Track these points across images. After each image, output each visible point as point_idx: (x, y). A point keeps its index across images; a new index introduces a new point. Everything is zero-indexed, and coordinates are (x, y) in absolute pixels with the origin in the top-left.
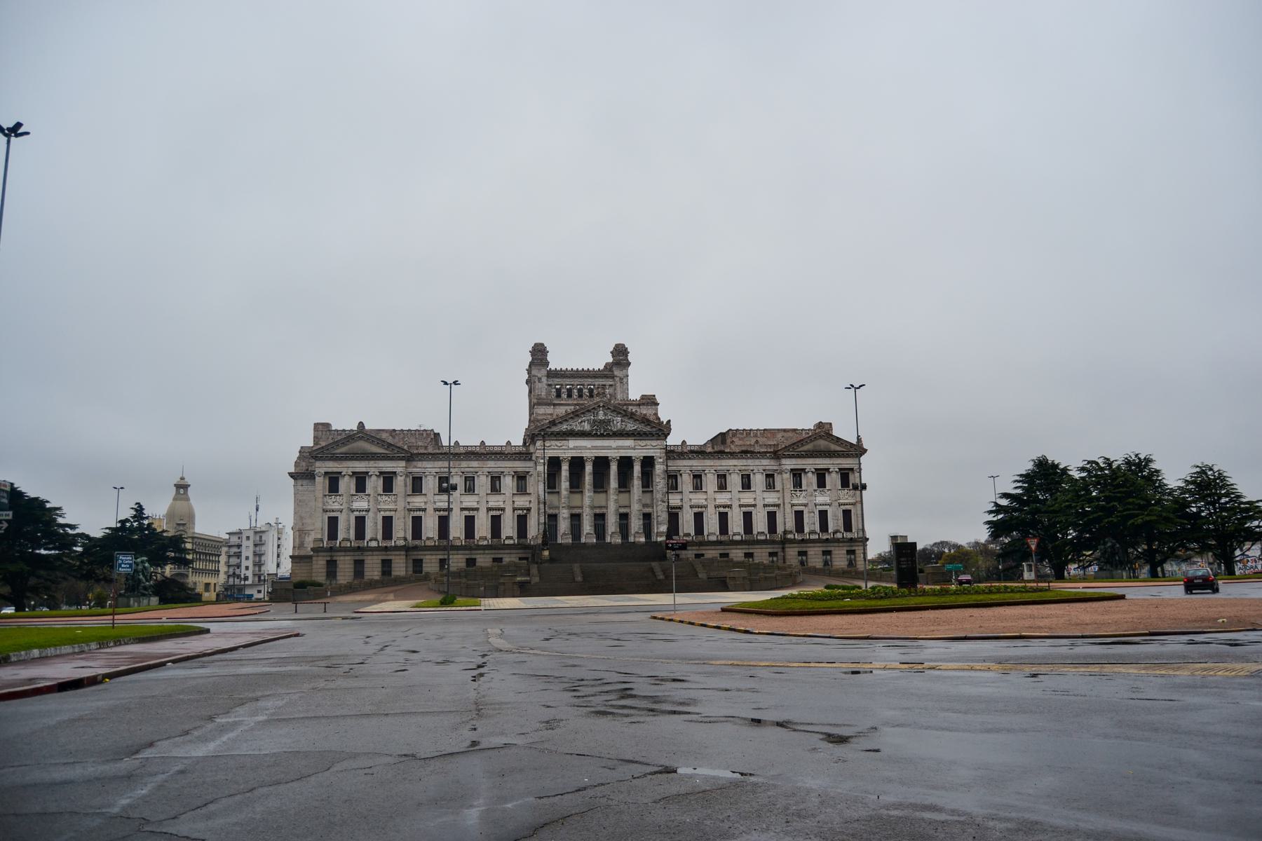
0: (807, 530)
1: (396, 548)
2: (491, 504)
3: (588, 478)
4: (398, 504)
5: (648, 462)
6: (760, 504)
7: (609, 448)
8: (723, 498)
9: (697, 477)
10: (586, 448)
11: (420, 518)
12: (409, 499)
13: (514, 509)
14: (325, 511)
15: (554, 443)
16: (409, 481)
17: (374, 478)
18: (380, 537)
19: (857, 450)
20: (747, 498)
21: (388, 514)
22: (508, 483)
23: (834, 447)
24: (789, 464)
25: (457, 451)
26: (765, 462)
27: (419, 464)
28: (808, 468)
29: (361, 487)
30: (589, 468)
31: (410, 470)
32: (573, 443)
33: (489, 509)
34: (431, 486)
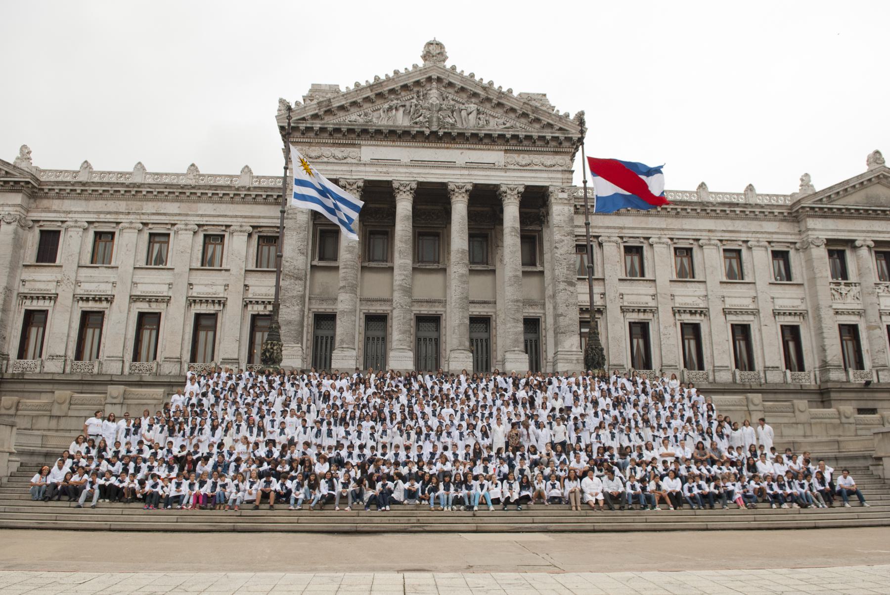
2: (197, 291)
3: (403, 227)
5: (535, 202)
6: (766, 310)
7: (450, 165)
8: (688, 295)
9: (634, 251)
10: (396, 163)
12: (26, 274)
15: (327, 151)
16: (32, 239)
20: (739, 297)
22: (238, 249)
24: (823, 229)
25: (138, 180)
26: (771, 226)
27: (56, 204)
28: (860, 239)
30: (404, 206)
31: (35, 215)
32: (368, 151)
33: (192, 301)
34: (76, 250)
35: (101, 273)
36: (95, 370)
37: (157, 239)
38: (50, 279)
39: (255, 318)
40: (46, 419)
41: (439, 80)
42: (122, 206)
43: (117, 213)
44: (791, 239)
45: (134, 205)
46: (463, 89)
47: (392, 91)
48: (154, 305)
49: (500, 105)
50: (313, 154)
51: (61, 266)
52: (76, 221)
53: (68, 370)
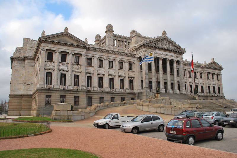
0: (211, 93)
1: (82, 91)
2: (120, 74)
4: (82, 69)
7: (167, 55)
11: (91, 77)
13: (129, 77)
14: (46, 69)
17: (71, 55)
18: (73, 84)
19: (220, 69)
21: (77, 74)
22: (126, 66)
23: (216, 67)
24: (207, 70)
26: (200, 69)
27: (91, 52)
29: (64, 59)
33: (119, 76)
35: (101, 69)
36: (104, 90)
37: (110, 62)
38: (92, 69)
39: (130, 80)
40: (156, 102)
41: (166, 39)
42: (104, 54)
43: (104, 56)
44: (202, 71)
45: (107, 54)
46: (169, 41)
47: (160, 40)
48: (112, 77)
49: (174, 45)
50: (148, 50)
51: (93, 67)
52: (96, 57)
53: (99, 90)
